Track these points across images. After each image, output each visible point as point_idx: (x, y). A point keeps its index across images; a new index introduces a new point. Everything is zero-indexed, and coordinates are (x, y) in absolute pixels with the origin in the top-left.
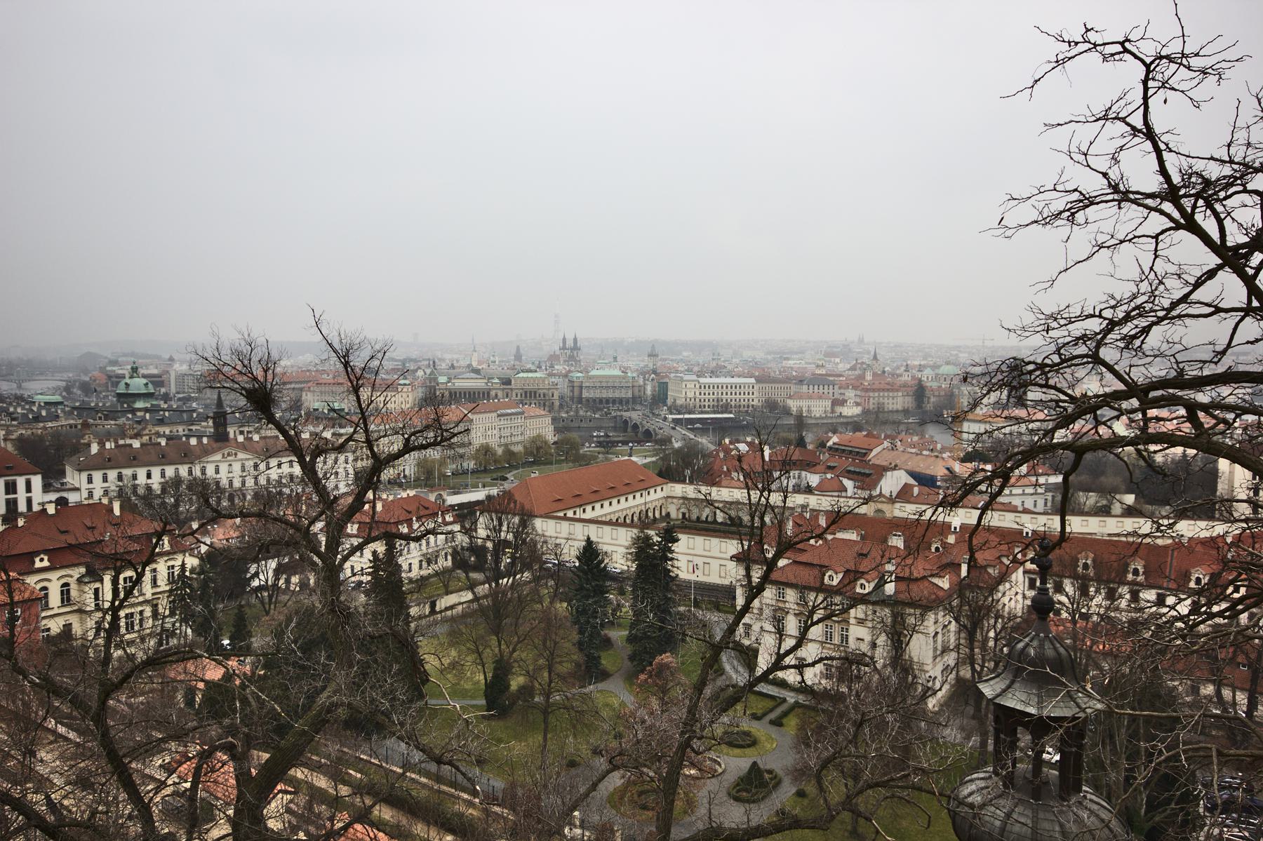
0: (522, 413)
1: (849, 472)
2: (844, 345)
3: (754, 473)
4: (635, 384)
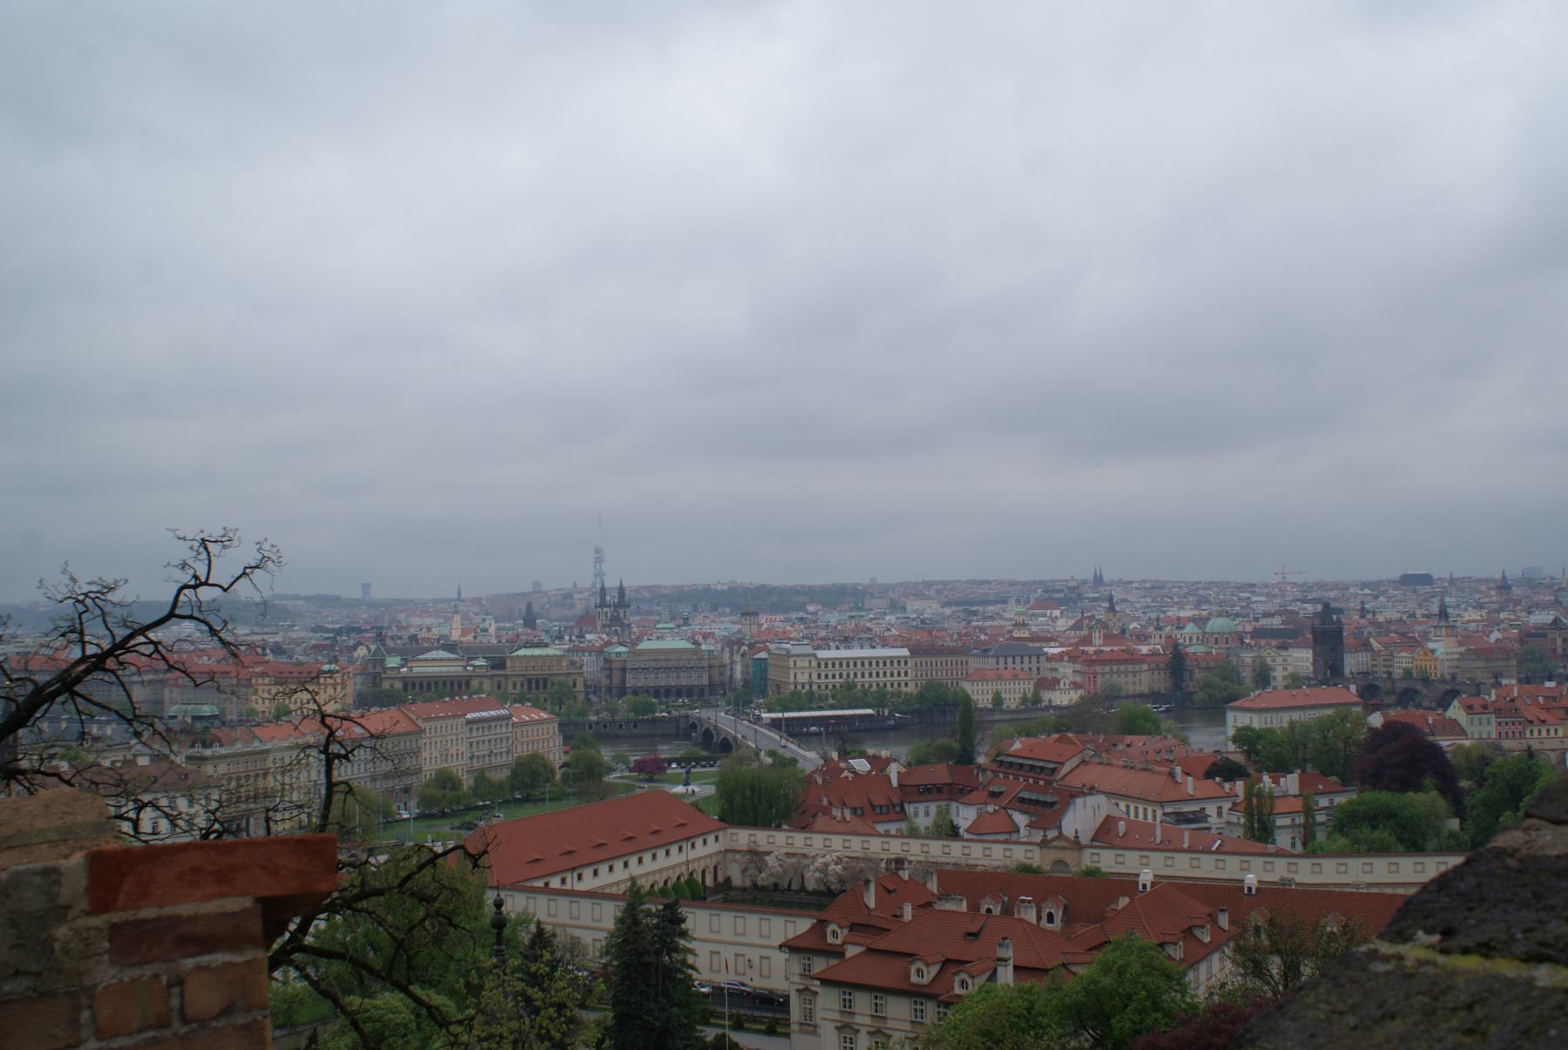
0: (509, 717)
1: (1022, 800)
2: (1071, 589)
3: (873, 807)
4: (715, 662)
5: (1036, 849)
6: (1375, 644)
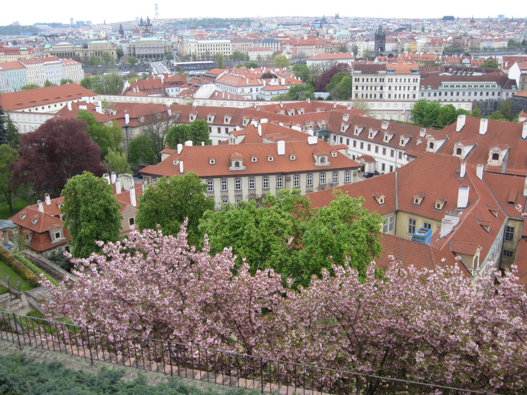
3: (154, 89)
5: (182, 99)
6: (399, 40)
